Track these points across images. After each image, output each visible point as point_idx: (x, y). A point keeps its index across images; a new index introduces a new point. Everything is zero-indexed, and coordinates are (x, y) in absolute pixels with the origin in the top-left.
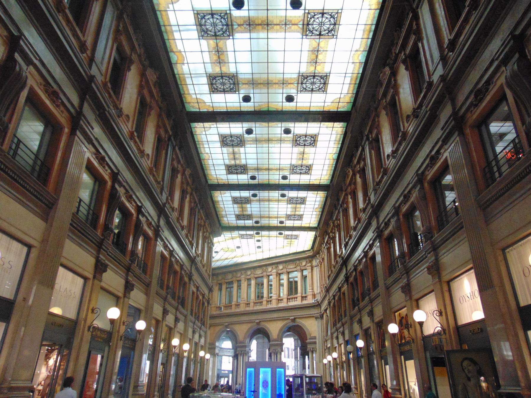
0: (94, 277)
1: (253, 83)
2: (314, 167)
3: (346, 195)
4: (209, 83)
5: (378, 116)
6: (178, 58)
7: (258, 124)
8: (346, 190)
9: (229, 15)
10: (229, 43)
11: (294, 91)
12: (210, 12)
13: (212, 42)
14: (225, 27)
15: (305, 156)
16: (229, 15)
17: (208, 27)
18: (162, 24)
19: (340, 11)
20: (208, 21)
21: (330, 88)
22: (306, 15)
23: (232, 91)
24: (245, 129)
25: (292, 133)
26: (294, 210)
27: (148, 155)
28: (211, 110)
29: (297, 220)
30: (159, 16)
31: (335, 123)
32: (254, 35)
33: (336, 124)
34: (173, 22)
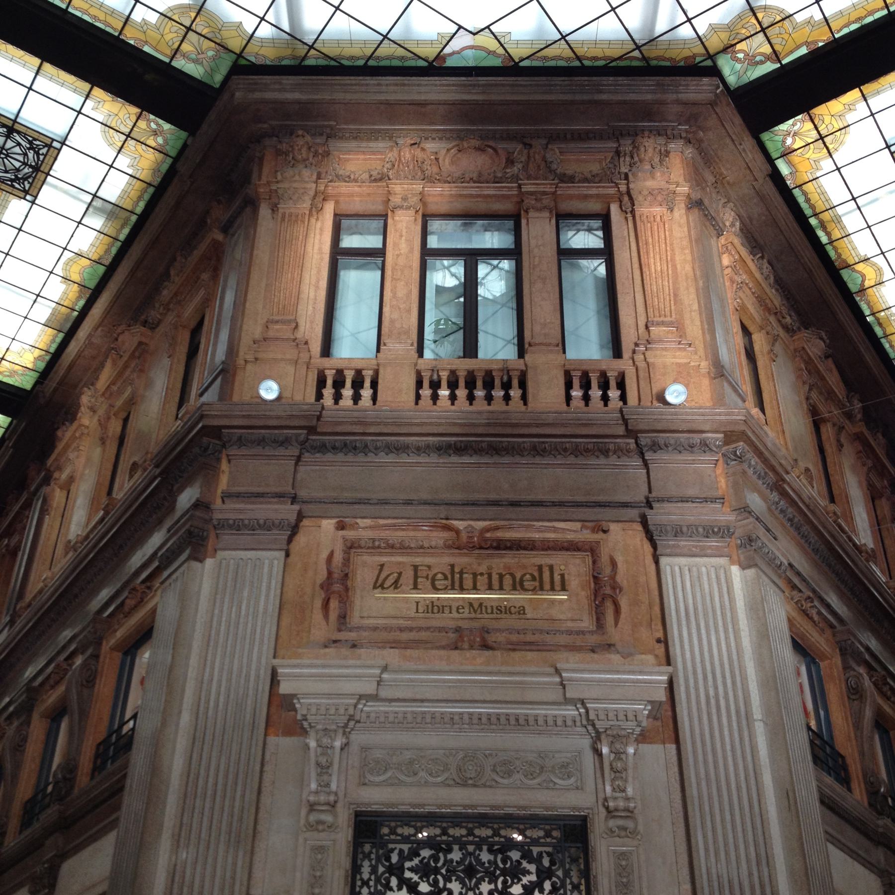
6: (863, 276)
18: (808, 212)
27: (872, 550)
30: (801, 200)
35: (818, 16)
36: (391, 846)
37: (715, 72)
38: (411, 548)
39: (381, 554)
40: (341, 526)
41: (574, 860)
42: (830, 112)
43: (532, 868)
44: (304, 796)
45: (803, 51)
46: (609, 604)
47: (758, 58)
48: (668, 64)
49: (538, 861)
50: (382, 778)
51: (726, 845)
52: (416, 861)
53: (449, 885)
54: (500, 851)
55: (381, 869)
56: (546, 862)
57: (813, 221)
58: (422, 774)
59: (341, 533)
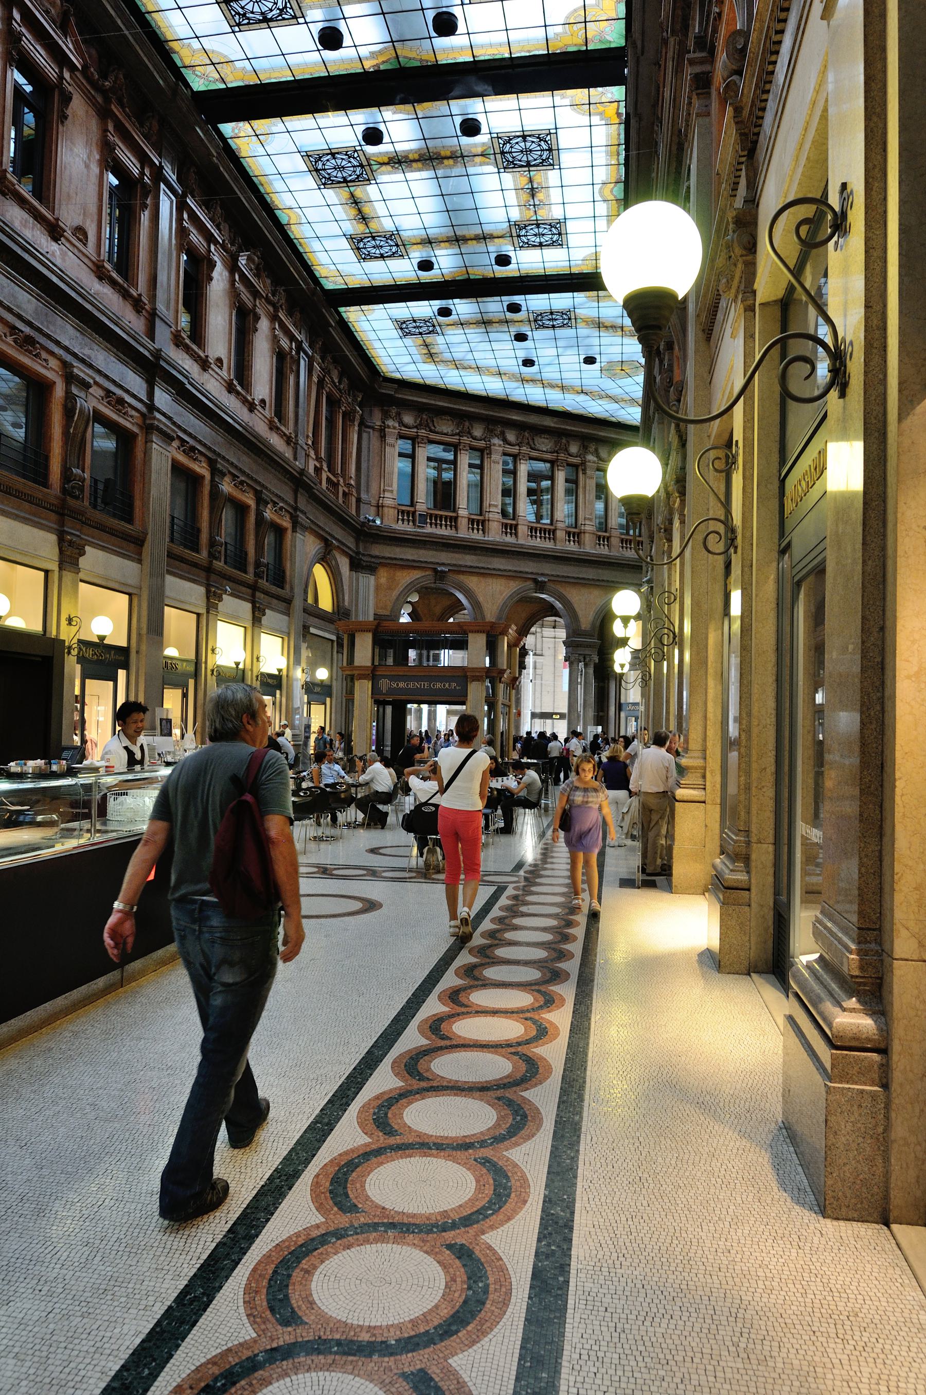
0: (208, 612)
4: (354, 247)
7: (456, 301)
9: (360, 153)
10: (372, 190)
12: (328, 152)
13: (344, 193)
14: (358, 169)
16: (360, 153)
17: (329, 171)
20: (328, 163)
21: (572, 240)
24: (436, 309)
25: (524, 308)
28: (368, 284)
32: (410, 175)
34: (270, 170)
35: (249, 68)
42: (261, 125)
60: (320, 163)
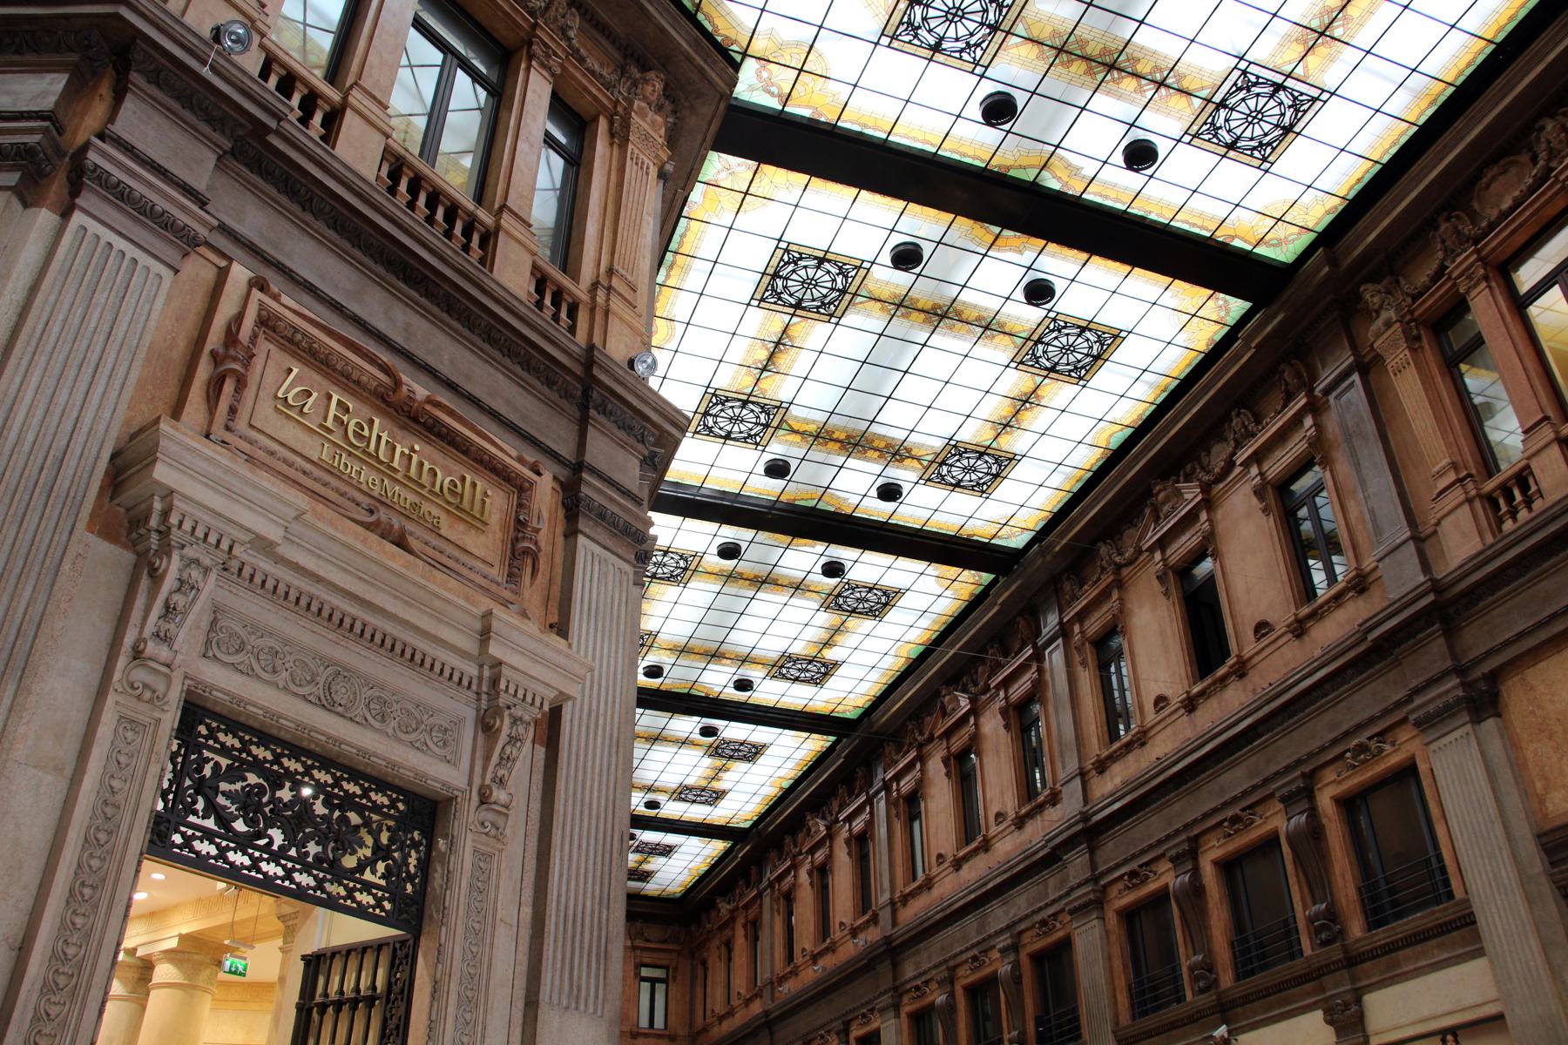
1: (821, 436)
2: (841, 671)
3: (921, 759)
5: (1119, 584)
7: (763, 536)
8: (920, 746)
11: (914, 477)
13: (777, 321)
15: (837, 638)
18: (673, 246)
19: (1123, 334)
22: (1047, 321)
23: (748, 438)
24: (719, 541)
26: (711, 773)
29: (706, 802)
31: (966, 572)
33: (968, 575)
36: (206, 753)
37: (737, 67)
38: (335, 370)
39: (294, 355)
40: (260, 284)
41: (415, 845)
43: (369, 841)
44: (129, 638)
45: (807, 113)
46: (529, 562)
47: (774, 89)
48: (710, 29)
49: (376, 836)
50: (230, 659)
51: (578, 875)
52: (238, 786)
53: (270, 832)
54: (339, 807)
55: (188, 782)
56: (384, 838)
57: (669, 256)
58: (285, 675)
59: (257, 294)
60: (791, 267)
